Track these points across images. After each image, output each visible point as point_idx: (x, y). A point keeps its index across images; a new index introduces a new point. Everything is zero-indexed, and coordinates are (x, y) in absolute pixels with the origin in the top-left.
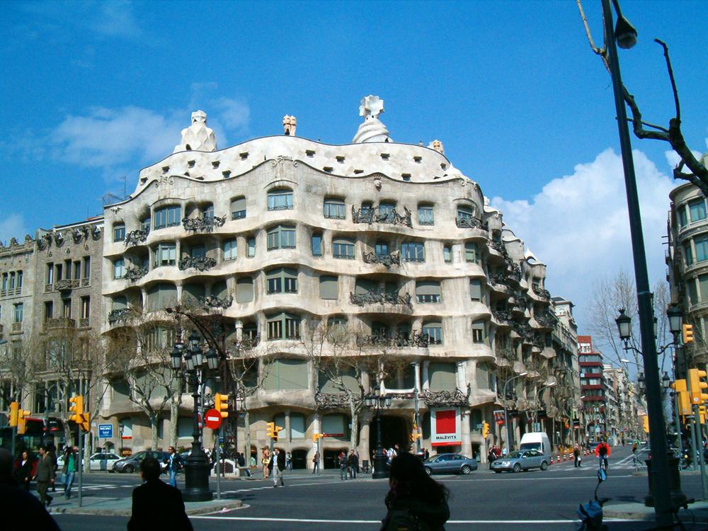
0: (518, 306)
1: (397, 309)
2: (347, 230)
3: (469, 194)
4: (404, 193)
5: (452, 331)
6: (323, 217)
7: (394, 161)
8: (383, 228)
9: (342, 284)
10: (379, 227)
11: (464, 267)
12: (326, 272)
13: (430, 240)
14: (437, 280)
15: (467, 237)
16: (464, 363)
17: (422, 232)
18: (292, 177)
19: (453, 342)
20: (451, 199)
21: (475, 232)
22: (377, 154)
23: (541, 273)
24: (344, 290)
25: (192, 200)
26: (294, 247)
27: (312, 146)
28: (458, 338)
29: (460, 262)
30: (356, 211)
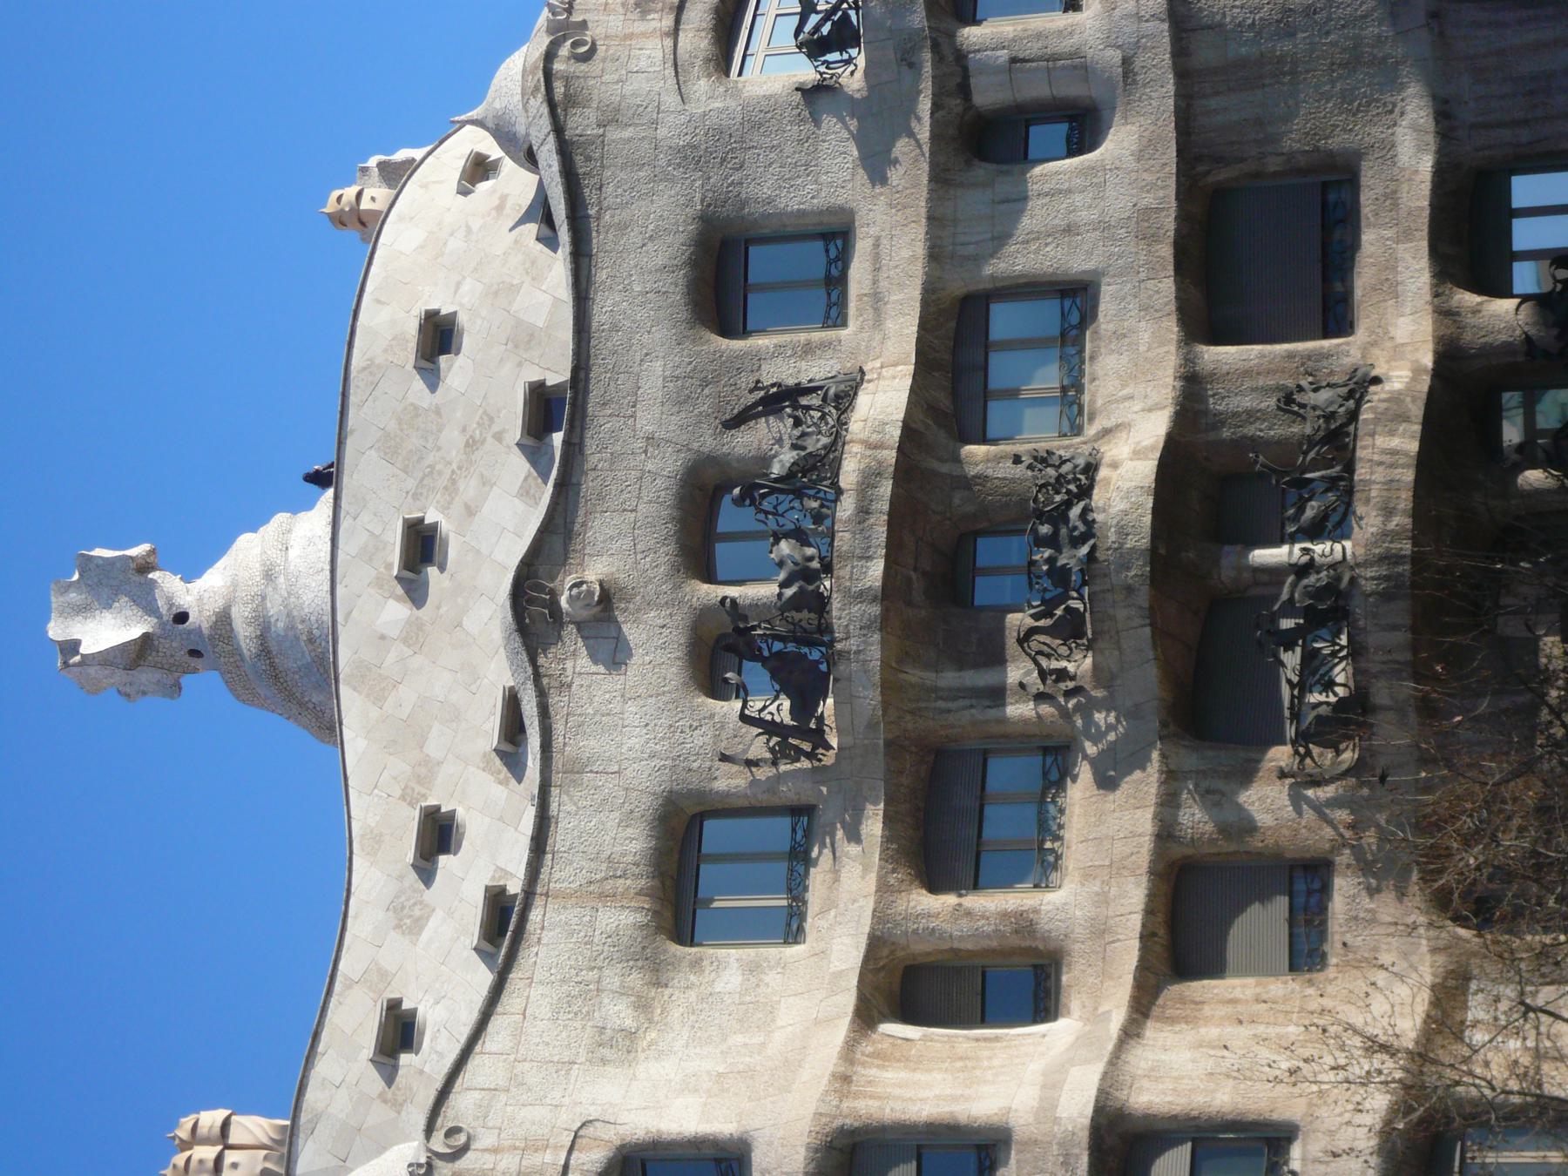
4: (646, 421)
7: (452, 488)
12: (1146, 937)
13: (935, 255)
27: (353, 1023)
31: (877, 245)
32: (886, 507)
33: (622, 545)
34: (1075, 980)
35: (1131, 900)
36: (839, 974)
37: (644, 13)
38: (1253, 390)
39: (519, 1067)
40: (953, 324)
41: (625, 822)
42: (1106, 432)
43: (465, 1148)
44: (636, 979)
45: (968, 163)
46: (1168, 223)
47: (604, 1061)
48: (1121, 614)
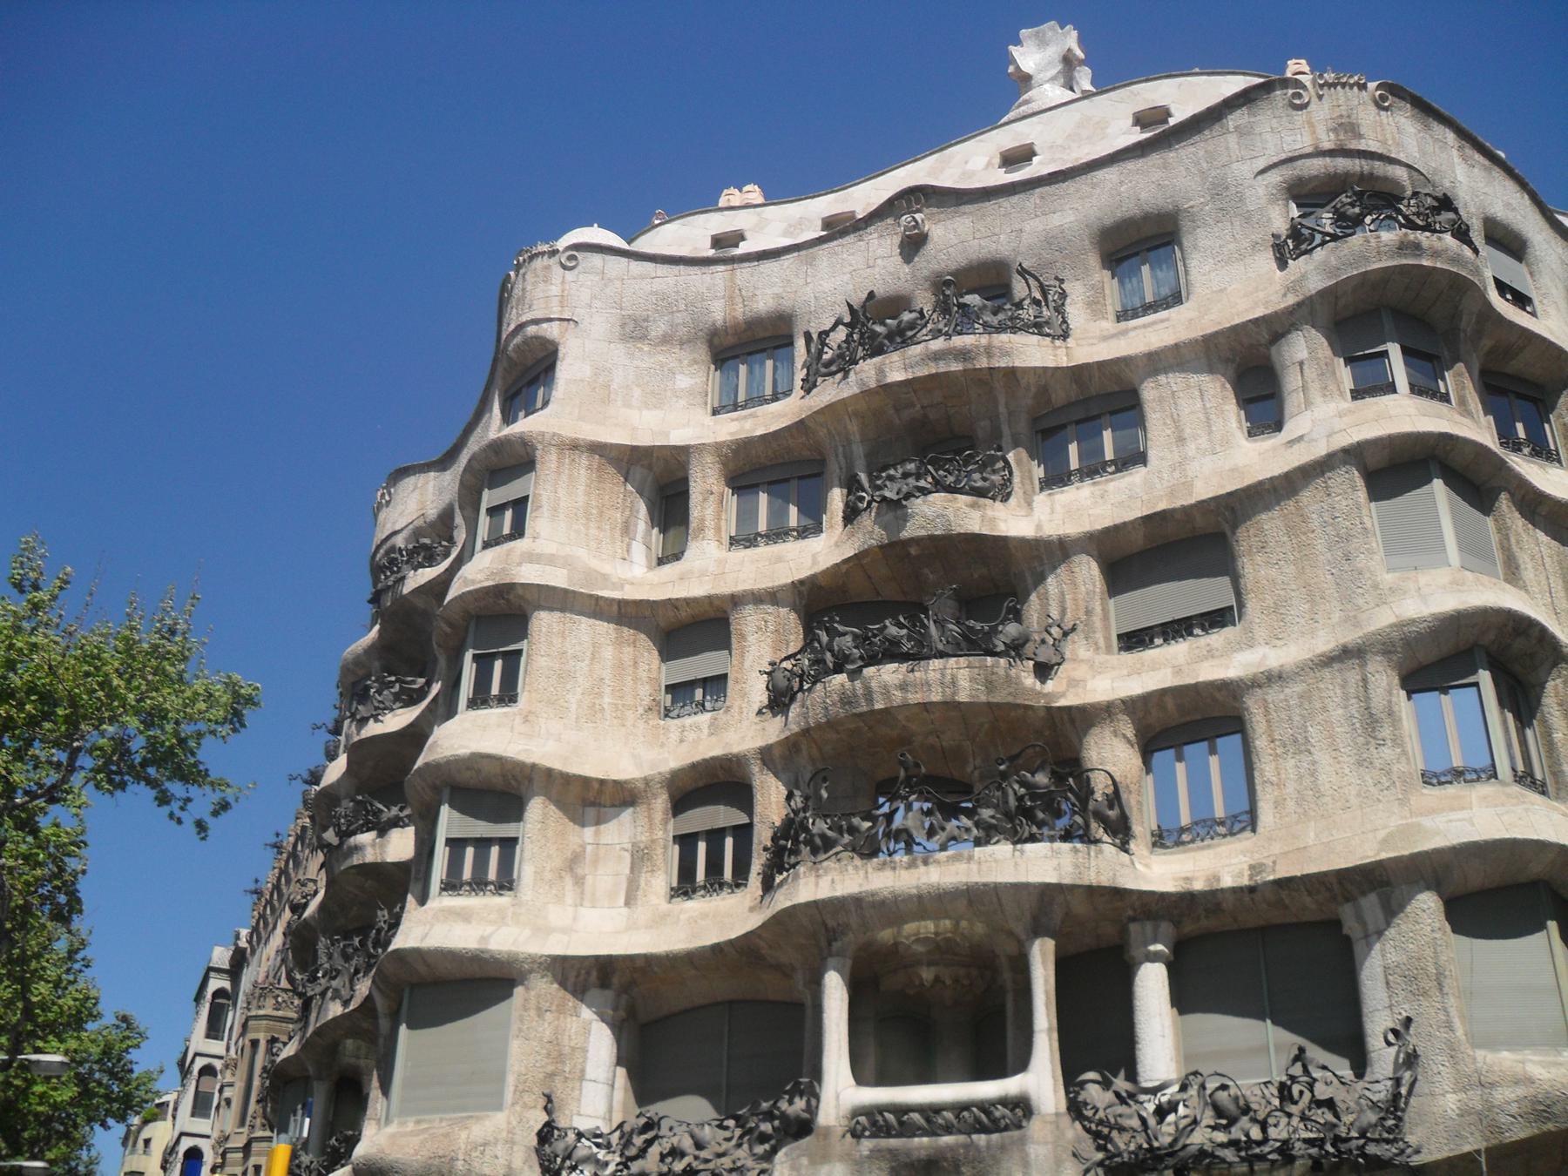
1: (953, 678)
5: (1300, 745)
8: (896, 368)
9: (743, 637)
10: (880, 371)
12: (672, 604)
15: (1316, 284)
16: (1370, 903)
17: (1113, 343)
18: (555, 302)
20: (1244, 170)
21: (1376, 246)
22: (989, 164)
24: (747, 664)
28: (1326, 776)
29: (1308, 404)
31: (1162, 321)
32: (941, 370)
33: (954, 239)
35: (697, 589)
36: (667, 434)
37: (1334, 130)
38: (1062, 594)
39: (618, 284)
40: (1117, 389)
41: (778, 296)
42: (1029, 504)
43: (564, 267)
44: (682, 331)
46: (1178, 504)
47: (623, 326)
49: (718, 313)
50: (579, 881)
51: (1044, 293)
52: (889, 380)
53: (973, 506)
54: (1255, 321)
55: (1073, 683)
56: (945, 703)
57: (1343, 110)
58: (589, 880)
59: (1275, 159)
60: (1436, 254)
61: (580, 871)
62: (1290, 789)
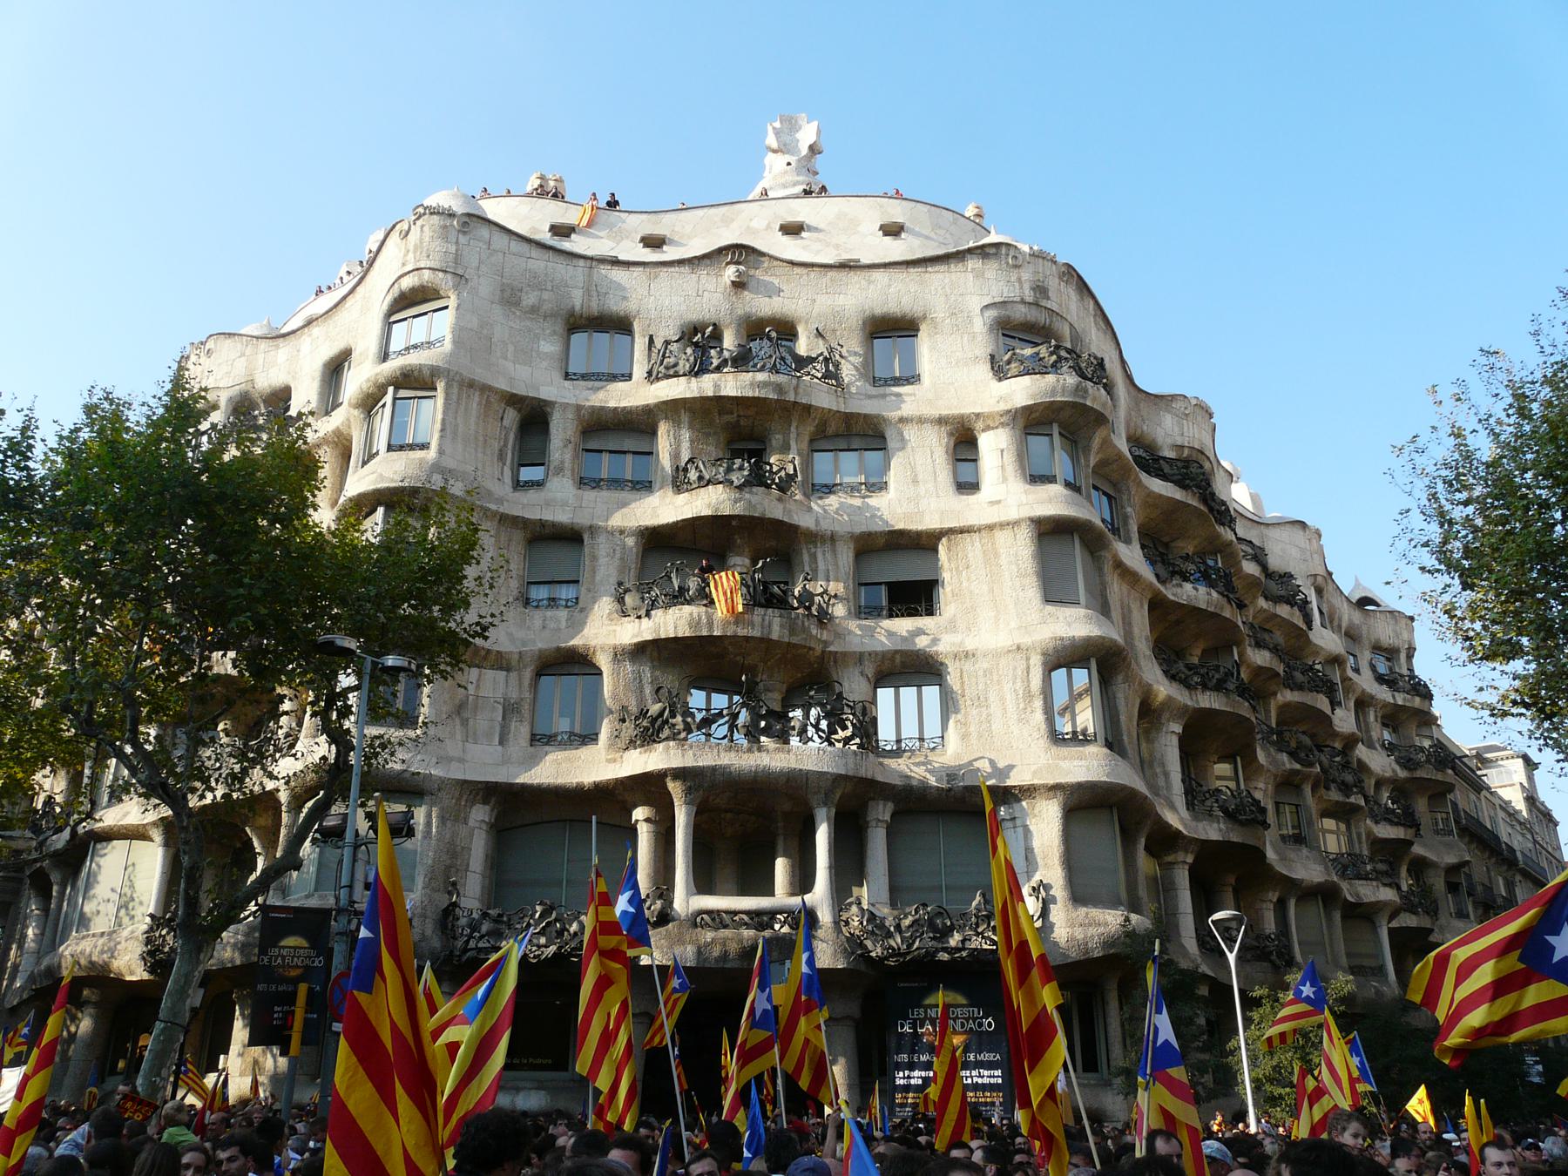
0: (1300, 688)
2: (623, 404)
3: (1041, 290)
6: (557, 377)
8: (732, 384)
9: (594, 558)
10: (717, 386)
11: (1009, 495)
13: (902, 420)
14: (924, 541)
17: (875, 402)
19: (980, 736)
22: (768, 227)
23: (1397, 635)
24: (598, 578)
25: (249, 387)
26: (424, 446)
30: (659, 343)
34: (532, 495)
35: (562, 517)
37: (1033, 289)
44: (546, 307)
45: (951, 434)
48: (699, 503)
49: (577, 300)
50: (465, 722)
51: (831, 350)
52: (723, 393)
53: (780, 499)
54: (978, 415)
55: (838, 635)
56: (761, 640)
57: (1041, 277)
58: (471, 722)
59: (997, 300)
60: (1094, 399)
61: (465, 715)
62: (972, 729)
